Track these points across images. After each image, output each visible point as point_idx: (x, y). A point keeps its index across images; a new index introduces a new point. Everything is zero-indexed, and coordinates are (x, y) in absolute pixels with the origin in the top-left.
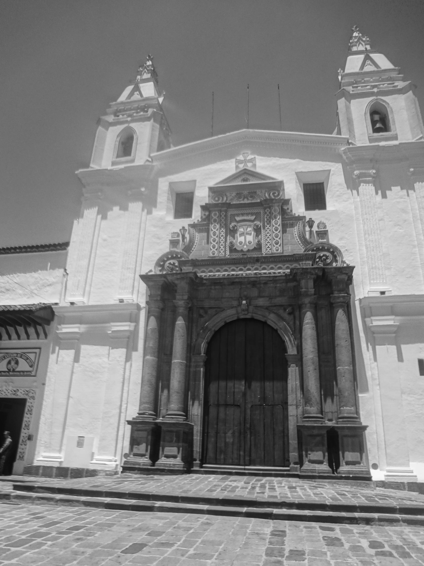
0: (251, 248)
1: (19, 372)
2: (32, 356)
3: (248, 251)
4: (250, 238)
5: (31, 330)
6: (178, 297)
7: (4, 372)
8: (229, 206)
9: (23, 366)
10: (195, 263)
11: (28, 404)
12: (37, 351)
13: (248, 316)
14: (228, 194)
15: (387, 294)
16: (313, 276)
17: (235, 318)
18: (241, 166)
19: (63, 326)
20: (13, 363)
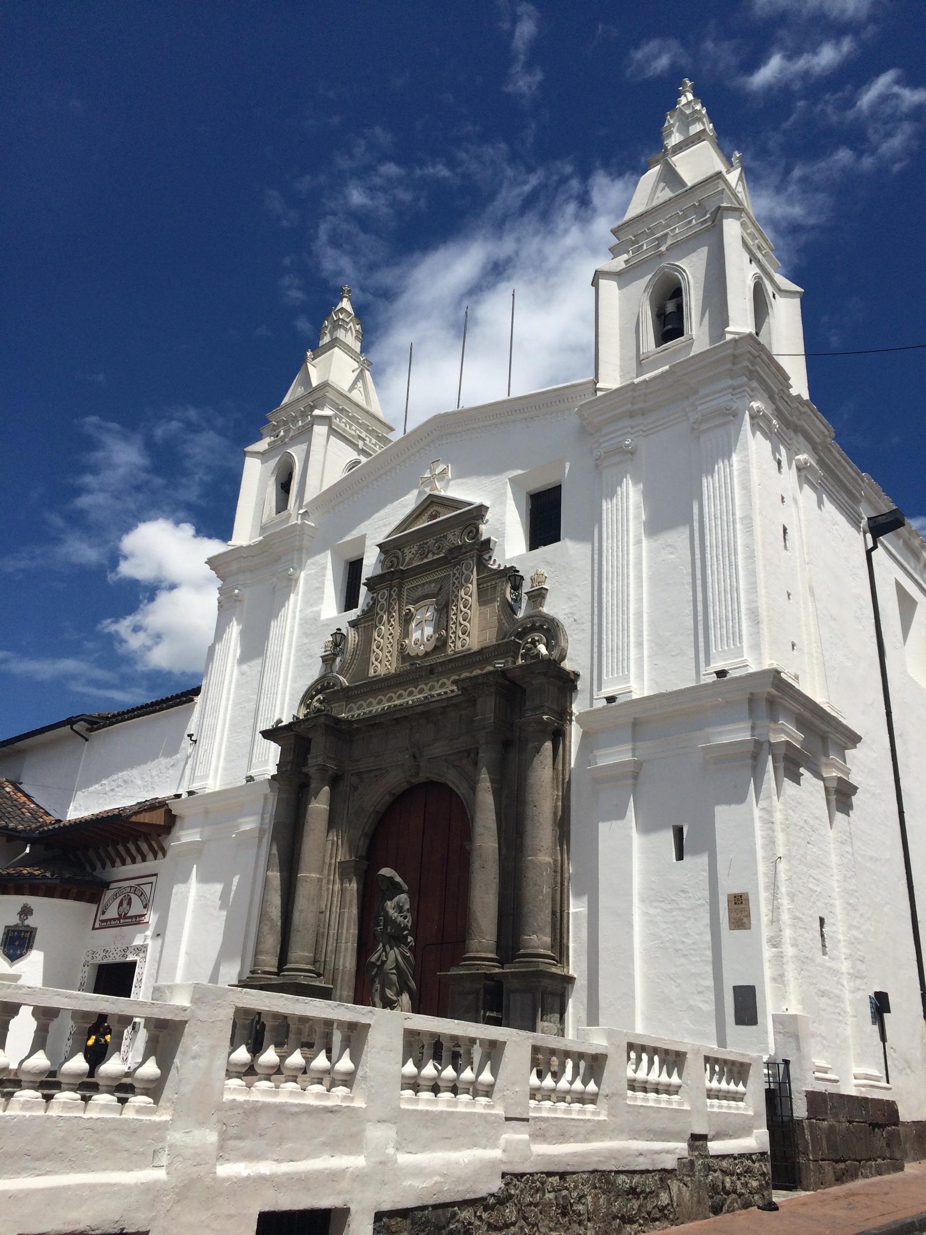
0: (429, 649)
1: (131, 917)
2: (147, 888)
3: (427, 654)
4: (429, 630)
5: (144, 847)
6: (310, 761)
7: (114, 919)
8: (403, 575)
9: (136, 908)
10: (347, 695)
11: (137, 970)
12: (153, 879)
13: (422, 778)
14: (406, 550)
15: (618, 702)
16: (493, 689)
17: (405, 786)
18: (428, 491)
19: (182, 833)
20: (125, 903)
